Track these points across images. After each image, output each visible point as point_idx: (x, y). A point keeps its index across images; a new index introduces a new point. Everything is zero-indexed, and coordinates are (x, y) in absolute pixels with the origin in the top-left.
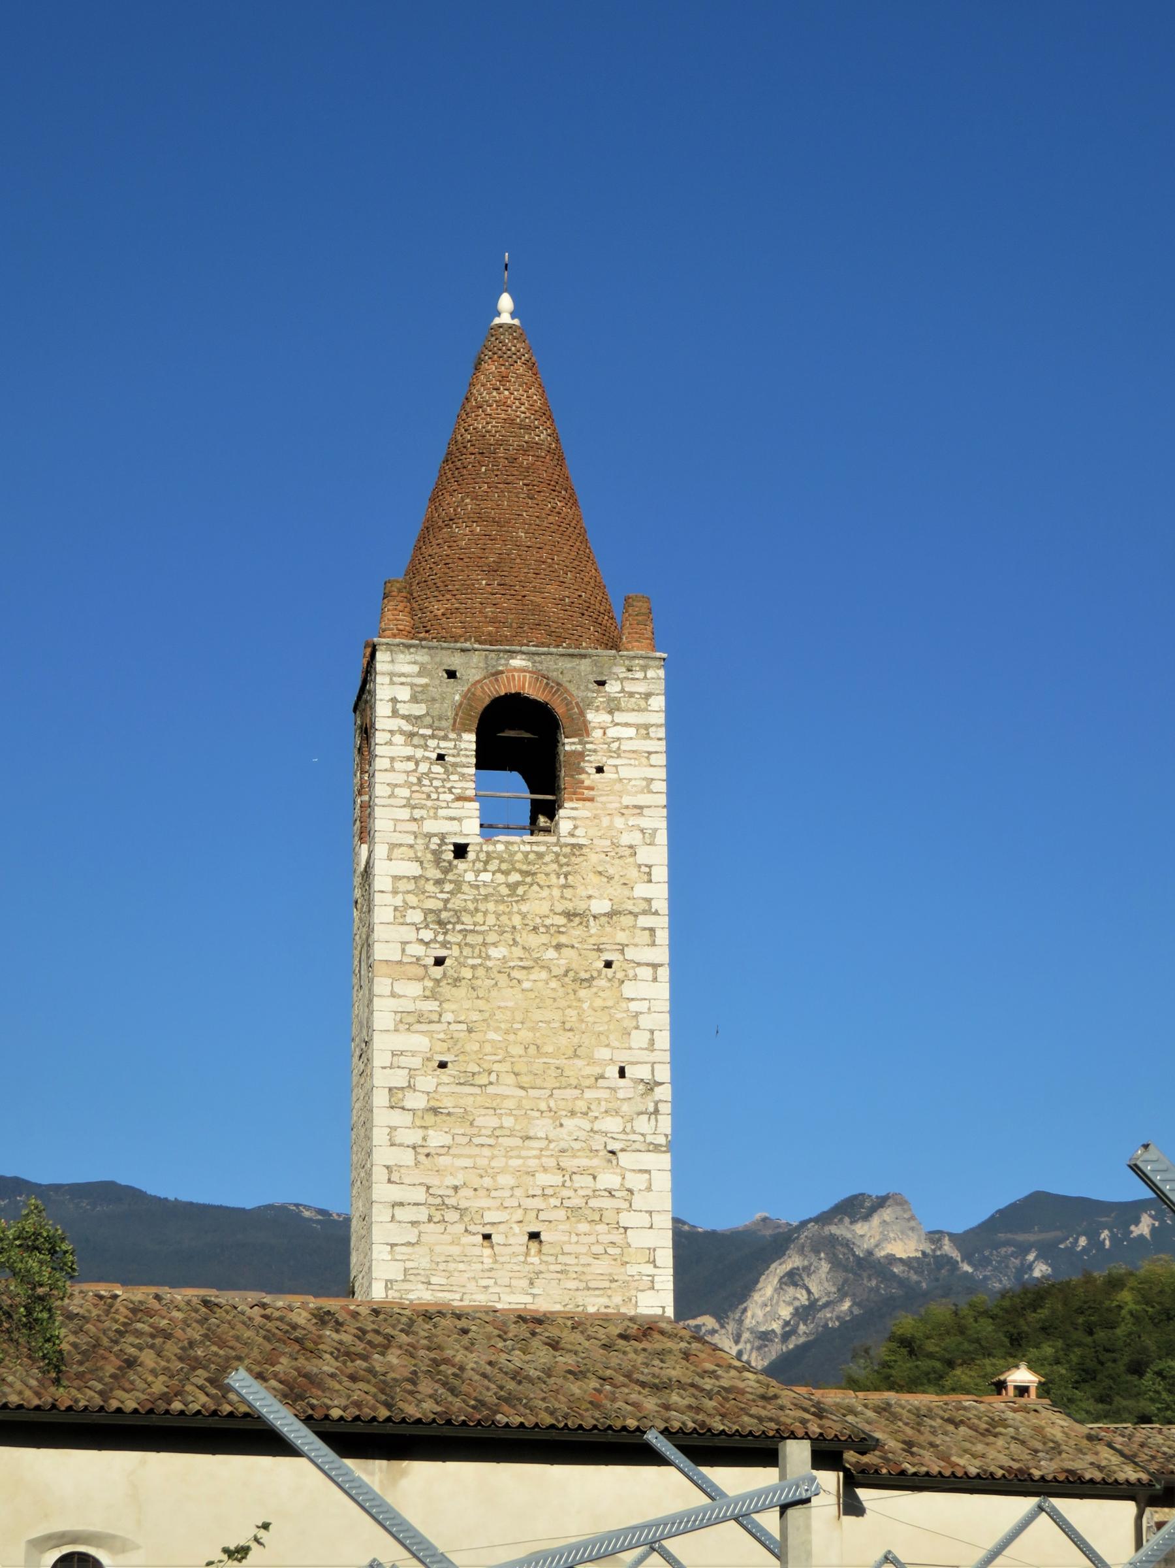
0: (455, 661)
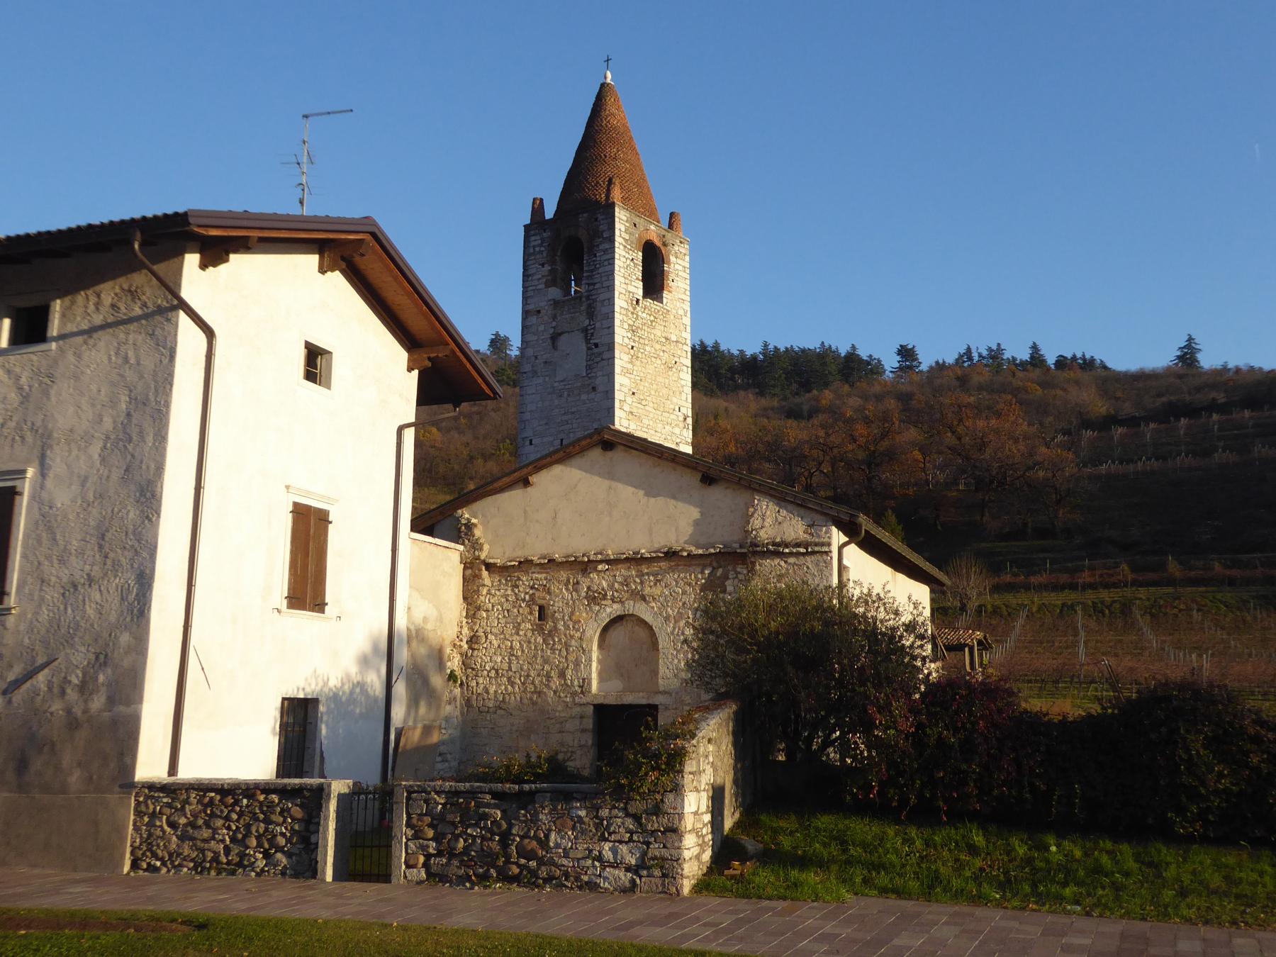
0: (637, 220)
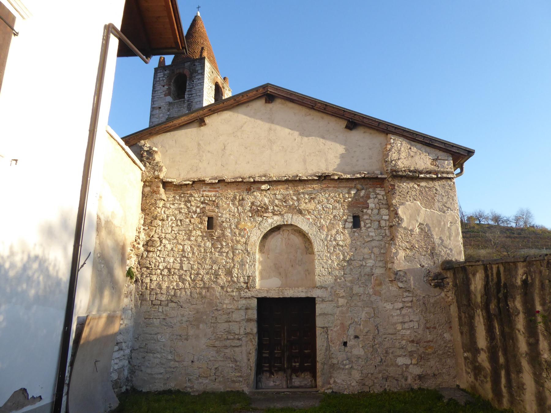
0: (214, 71)
